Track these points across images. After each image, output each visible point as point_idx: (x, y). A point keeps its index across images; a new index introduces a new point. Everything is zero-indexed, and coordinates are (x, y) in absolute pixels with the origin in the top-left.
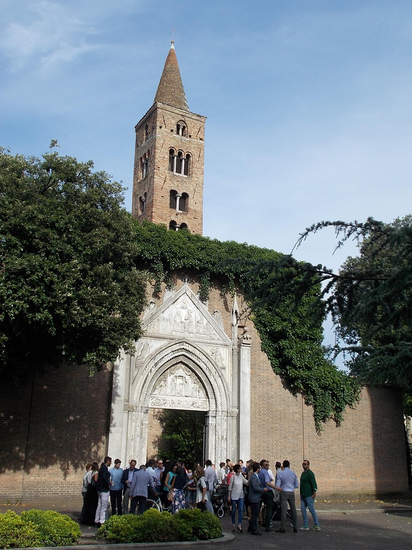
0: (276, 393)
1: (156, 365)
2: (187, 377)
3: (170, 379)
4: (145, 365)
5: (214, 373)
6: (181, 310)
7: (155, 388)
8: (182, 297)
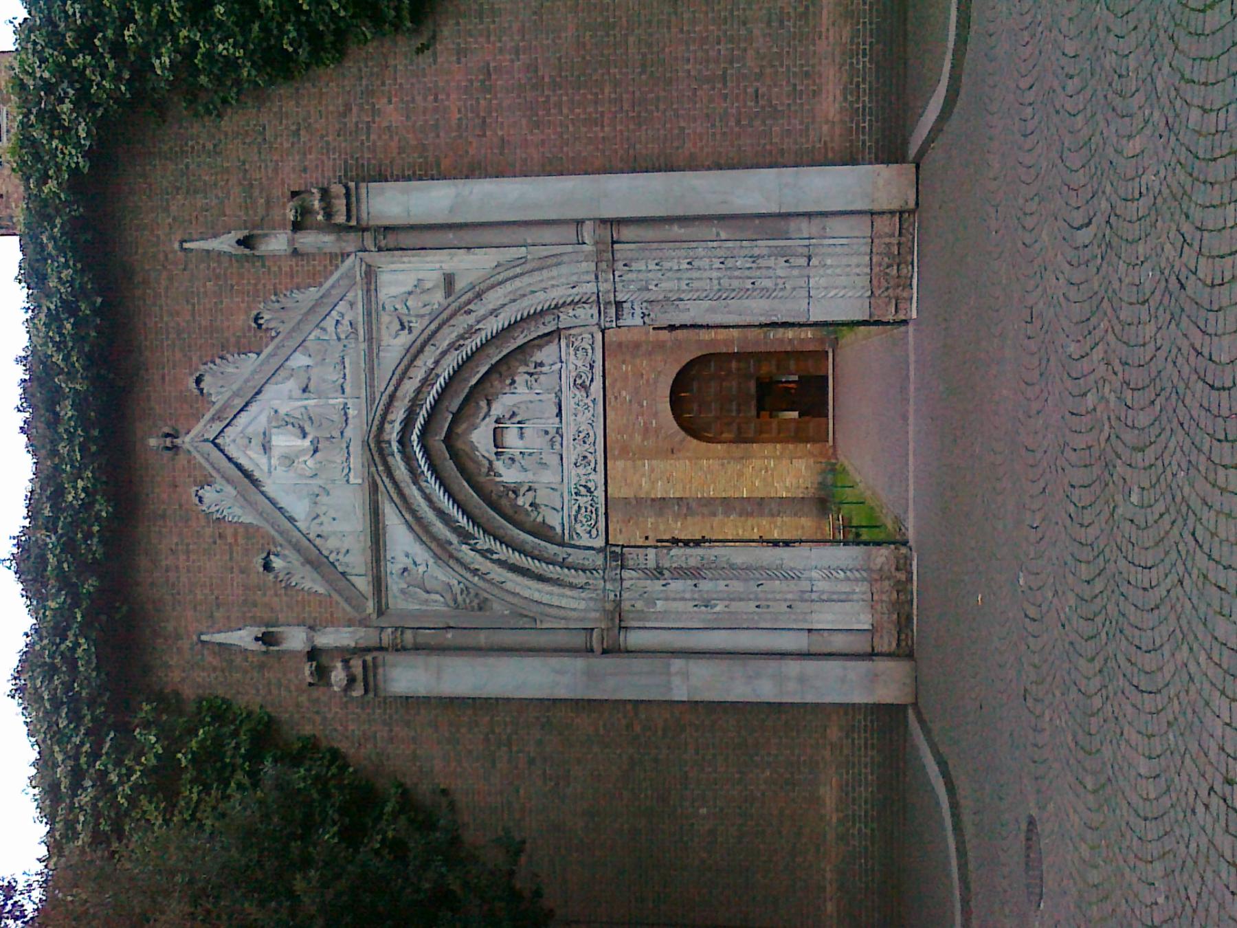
0: (517, 53)
1: (465, 537)
2: (498, 409)
3: (509, 475)
4: (468, 575)
5: (471, 319)
6: (276, 453)
7: (542, 532)
8: (233, 451)
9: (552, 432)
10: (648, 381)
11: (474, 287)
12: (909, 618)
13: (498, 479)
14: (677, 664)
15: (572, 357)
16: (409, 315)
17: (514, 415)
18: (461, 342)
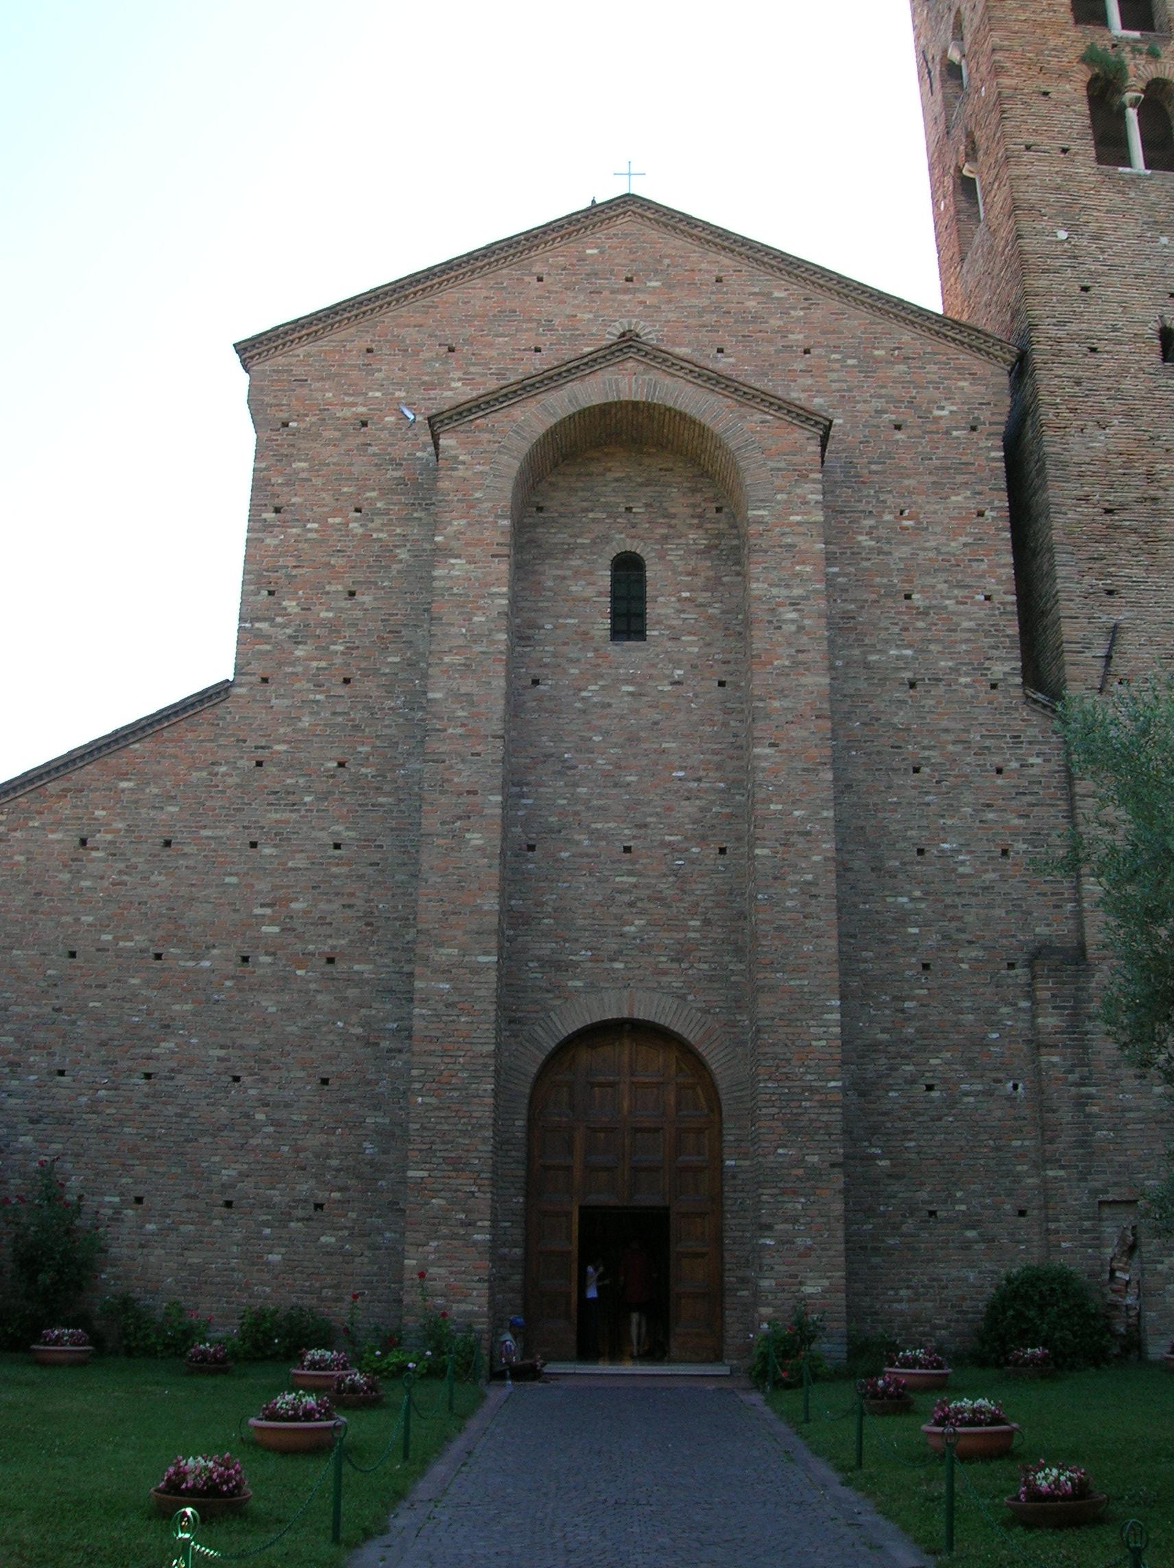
10: (665, 973)
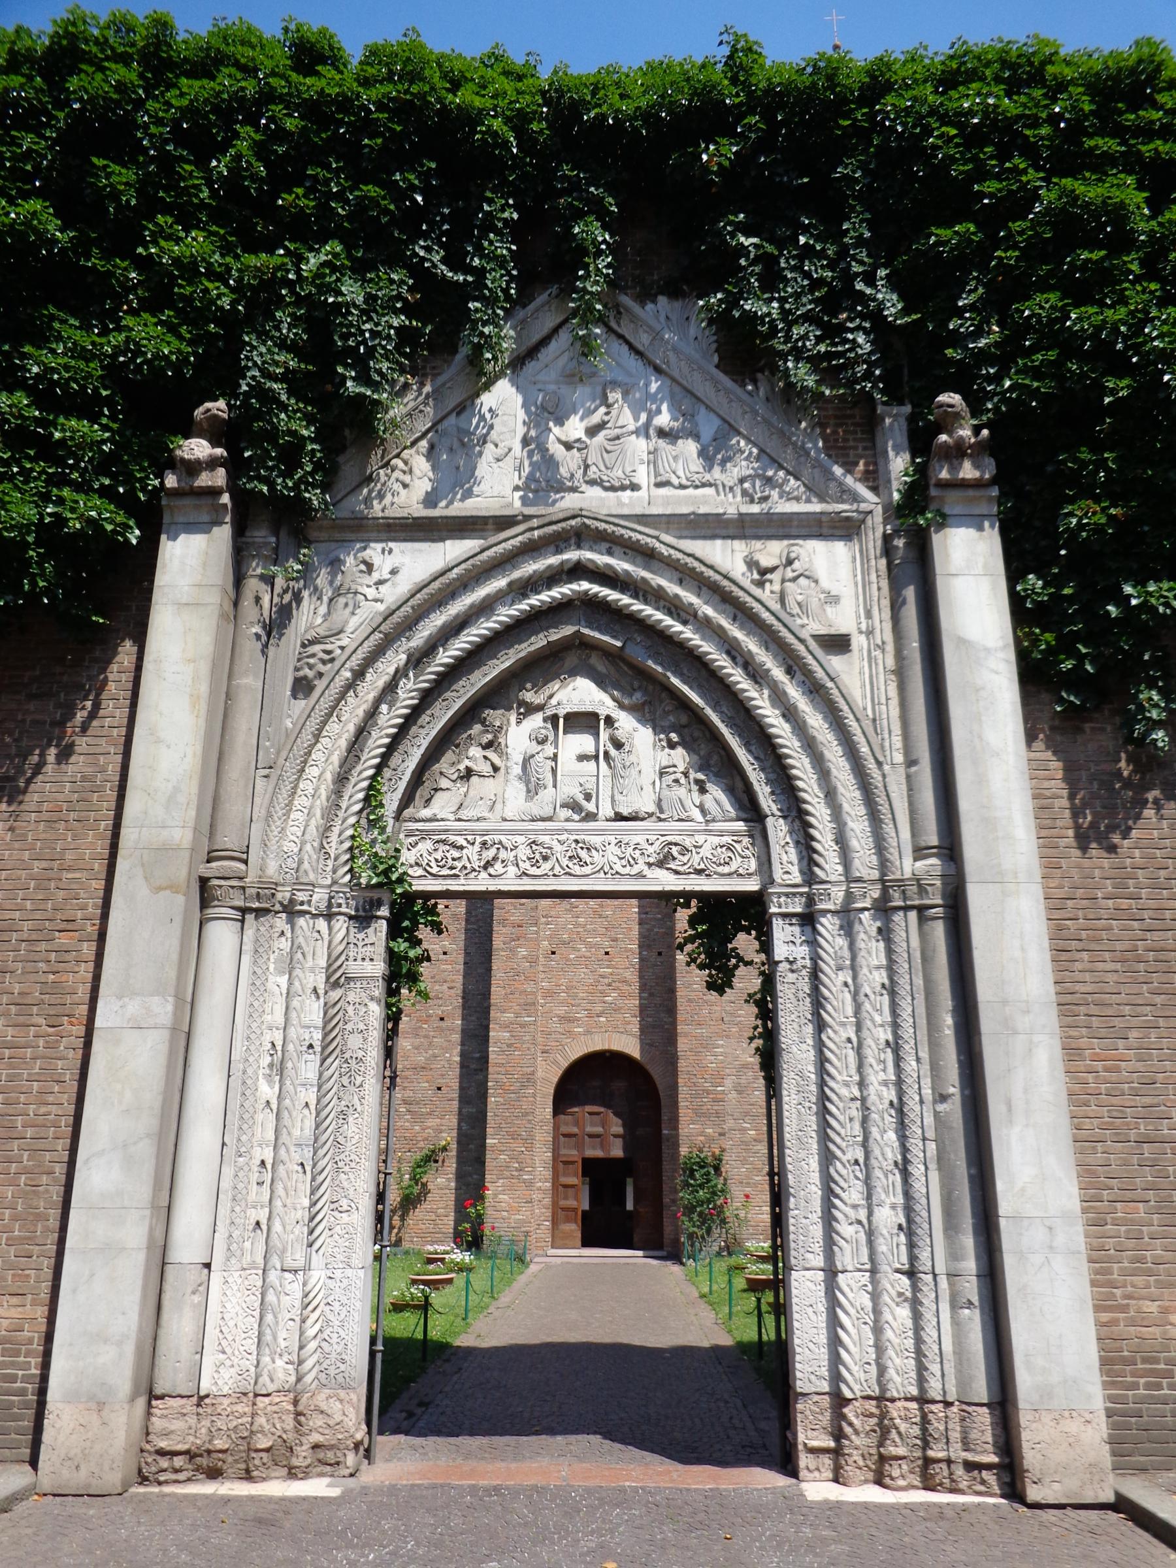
1: (418, 660)
4: (354, 662)
6: (564, 390)
9: (590, 807)
11: (832, 679)
12: (214, 1474)
13: (513, 718)
14: (163, 1009)
15: (716, 840)
16: (783, 581)
17: (618, 745)
18: (739, 659)
